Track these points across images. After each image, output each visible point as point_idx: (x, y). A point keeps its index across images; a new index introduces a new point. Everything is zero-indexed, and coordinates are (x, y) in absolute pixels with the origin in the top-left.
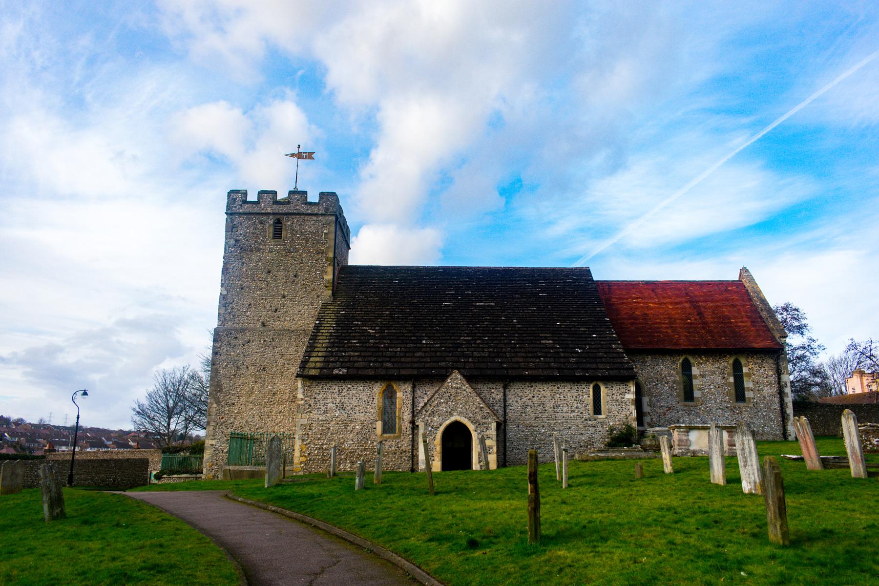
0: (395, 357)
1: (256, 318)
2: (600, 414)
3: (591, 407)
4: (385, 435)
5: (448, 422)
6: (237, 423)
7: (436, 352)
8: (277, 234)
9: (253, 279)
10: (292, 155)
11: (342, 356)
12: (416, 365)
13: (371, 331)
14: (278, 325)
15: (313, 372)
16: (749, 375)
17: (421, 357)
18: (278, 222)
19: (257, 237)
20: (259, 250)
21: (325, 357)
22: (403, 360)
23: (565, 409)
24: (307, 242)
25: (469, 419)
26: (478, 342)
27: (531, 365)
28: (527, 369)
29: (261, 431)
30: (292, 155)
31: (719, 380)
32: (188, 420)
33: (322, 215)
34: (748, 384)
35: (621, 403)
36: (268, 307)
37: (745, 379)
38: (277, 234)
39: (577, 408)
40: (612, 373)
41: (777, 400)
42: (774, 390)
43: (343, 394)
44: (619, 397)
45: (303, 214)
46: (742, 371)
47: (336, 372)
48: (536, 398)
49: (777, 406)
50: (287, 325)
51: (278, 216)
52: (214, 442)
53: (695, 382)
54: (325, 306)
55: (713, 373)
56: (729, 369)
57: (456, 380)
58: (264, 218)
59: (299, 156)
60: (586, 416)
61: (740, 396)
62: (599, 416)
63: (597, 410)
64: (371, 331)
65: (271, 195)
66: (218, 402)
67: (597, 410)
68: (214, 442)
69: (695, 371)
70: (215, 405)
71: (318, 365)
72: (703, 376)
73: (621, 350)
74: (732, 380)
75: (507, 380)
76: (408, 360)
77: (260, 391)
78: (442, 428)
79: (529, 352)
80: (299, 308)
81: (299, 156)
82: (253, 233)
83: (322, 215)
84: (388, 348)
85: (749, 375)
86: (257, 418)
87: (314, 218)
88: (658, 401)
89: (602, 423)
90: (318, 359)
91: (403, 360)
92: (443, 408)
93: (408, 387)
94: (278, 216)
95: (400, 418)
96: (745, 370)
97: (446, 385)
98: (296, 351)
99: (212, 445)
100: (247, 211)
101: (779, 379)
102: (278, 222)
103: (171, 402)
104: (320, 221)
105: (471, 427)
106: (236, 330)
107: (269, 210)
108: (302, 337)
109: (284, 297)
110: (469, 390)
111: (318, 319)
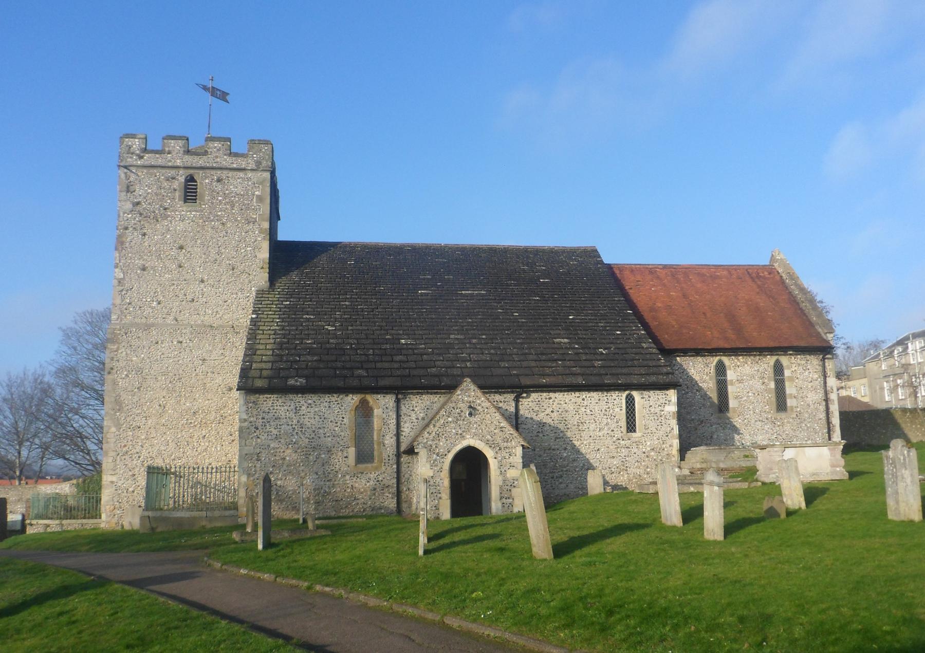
0: (368, 361)
2: (635, 431)
3: (623, 423)
4: (360, 466)
5: (459, 447)
6: (144, 453)
7: (422, 355)
8: (190, 192)
9: (159, 257)
10: (205, 88)
11: (296, 361)
12: (398, 373)
13: (330, 328)
14: (197, 320)
15: (259, 383)
16: (791, 379)
17: (403, 362)
18: (191, 179)
19: (162, 200)
20: (166, 217)
21: (273, 362)
22: (379, 365)
23: (592, 426)
24: (233, 207)
25: (487, 442)
26: (474, 341)
27: (547, 371)
28: (544, 375)
29: (179, 463)
30: (205, 88)
31: (757, 384)
32: (45, 447)
34: (790, 389)
35: (659, 416)
37: (787, 384)
38: (190, 192)
39: (607, 424)
40: (653, 379)
41: (822, 408)
42: (821, 395)
44: (657, 410)
45: (227, 169)
46: (783, 374)
47: (291, 382)
48: (555, 414)
49: (823, 416)
50: (208, 320)
51: (191, 172)
52: (114, 479)
53: (730, 389)
54: (260, 293)
55: (753, 377)
56: (770, 372)
57: (469, 393)
58: (172, 173)
59: (214, 92)
60: (618, 434)
61: (781, 405)
62: (633, 434)
63: (631, 426)
64: (330, 328)
65: (181, 143)
66: (118, 426)
67: (631, 426)
68: (114, 479)
69: (731, 375)
70: (113, 429)
71: (265, 373)
72: (740, 381)
73: (654, 351)
74: (772, 385)
75: (520, 390)
76: (386, 365)
77: (175, 410)
78: (450, 456)
79: (542, 354)
80: (225, 297)
81: (214, 92)
82: (156, 194)
84: (356, 350)
85: (791, 379)
86: (172, 445)
87: (241, 174)
88: (688, 413)
89: (638, 443)
90: (263, 366)
91: (379, 365)
92: (452, 430)
93: (388, 400)
94: (191, 172)
95: (379, 444)
96: (787, 373)
97: (454, 398)
98: (234, 355)
99: (112, 482)
100: (147, 163)
101: (825, 383)
102: (191, 179)
103: (21, 424)
104: (249, 179)
105: (489, 453)
106: (137, 325)
107: (179, 163)
108: (229, 336)
109: (202, 281)
110: (487, 404)
111: (254, 312)
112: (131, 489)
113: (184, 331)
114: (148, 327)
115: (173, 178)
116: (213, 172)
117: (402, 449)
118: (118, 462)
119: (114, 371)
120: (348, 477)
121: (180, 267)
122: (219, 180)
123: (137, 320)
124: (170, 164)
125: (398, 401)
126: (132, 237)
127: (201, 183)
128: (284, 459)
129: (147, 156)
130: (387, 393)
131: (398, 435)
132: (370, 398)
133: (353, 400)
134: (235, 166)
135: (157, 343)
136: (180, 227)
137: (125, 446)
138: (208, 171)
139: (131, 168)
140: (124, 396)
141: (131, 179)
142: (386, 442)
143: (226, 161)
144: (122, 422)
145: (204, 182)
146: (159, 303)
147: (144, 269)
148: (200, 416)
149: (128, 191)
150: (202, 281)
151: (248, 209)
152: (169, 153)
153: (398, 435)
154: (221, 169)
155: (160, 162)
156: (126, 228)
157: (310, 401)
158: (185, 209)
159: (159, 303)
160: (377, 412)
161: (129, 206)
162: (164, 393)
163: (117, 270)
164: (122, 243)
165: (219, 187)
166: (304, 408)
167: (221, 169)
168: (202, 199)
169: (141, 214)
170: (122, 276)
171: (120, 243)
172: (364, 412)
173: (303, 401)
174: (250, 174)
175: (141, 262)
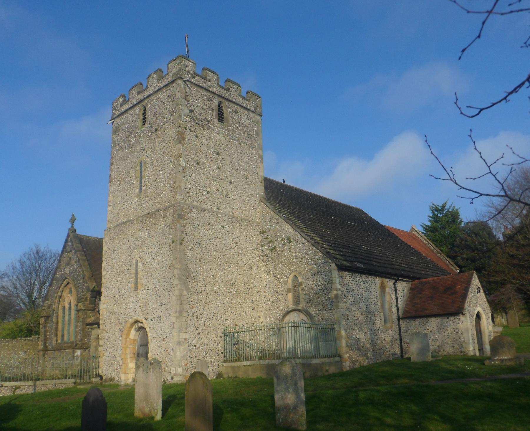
1: (212, 200)
18: (220, 106)
19: (206, 113)
20: (209, 128)
33: (253, 112)
36: (220, 190)
43: (362, 287)
47: (359, 265)
50: (237, 213)
51: (221, 100)
52: (187, 336)
58: (211, 96)
65: (216, 77)
83: (253, 112)
87: (246, 112)
99: (186, 339)
100: (198, 83)
104: (251, 117)
106: (197, 208)
107: (215, 90)
112: (198, 346)
113: (224, 218)
114: (204, 210)
115: (212, 101)
116: (233, 105)
117: (401, 316)
118: (189, 322)
119: (184, 243)
120: (382, 333)
121: (219, 168)
122: (236, 112)
123: (195, 203)
124: (210, 89)
125: (395, 284)
126: (189, 135)
127: (227, 110)
128: (358, 319)
129: (197, 78)
130: (390, 278)
131: (397, 306)
132: (386, 281)
133: (378, 280)
134: (244, 105)
135: (209, 224)
136: (218, 138)
137: (193, 308)
138: (230, 103)
139: (188, 83)
140: (190, 265)
141: (187, 91)
142: (393, 310)
143: (240, 101)
144: (190, 286)
145: (229, 110)
146: (208, 193)
147: (198, 164)
148: (236, 287)
149: (186, 100)
150: (231, 183)
151: (251, 138)
152: (210, 81)
153: (397, 306)
154: (237, 104)
155: (204, 85)
156: (185, 128)
157: (364, 280)
158: (219, 125)
159: (208, 193)
160: (387, 290)
161: (187, 111)
162: (215, 266)
163: (181, 159)
164: (184, 139)
165: (236, 117)
166: (362, 284)
167: (237, 104)
168: (228, 122)
169: (194, 120)
170: (184, 165)
171: (181, 138)
172: (383, 287)
173: (360, 278)
174: (251, 114)
175: (196, 158)
